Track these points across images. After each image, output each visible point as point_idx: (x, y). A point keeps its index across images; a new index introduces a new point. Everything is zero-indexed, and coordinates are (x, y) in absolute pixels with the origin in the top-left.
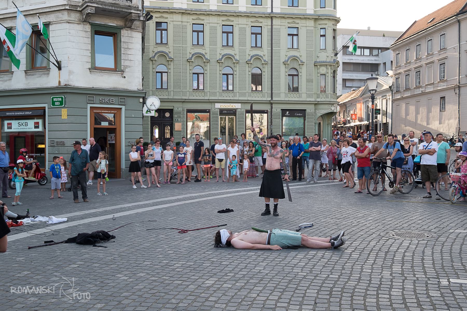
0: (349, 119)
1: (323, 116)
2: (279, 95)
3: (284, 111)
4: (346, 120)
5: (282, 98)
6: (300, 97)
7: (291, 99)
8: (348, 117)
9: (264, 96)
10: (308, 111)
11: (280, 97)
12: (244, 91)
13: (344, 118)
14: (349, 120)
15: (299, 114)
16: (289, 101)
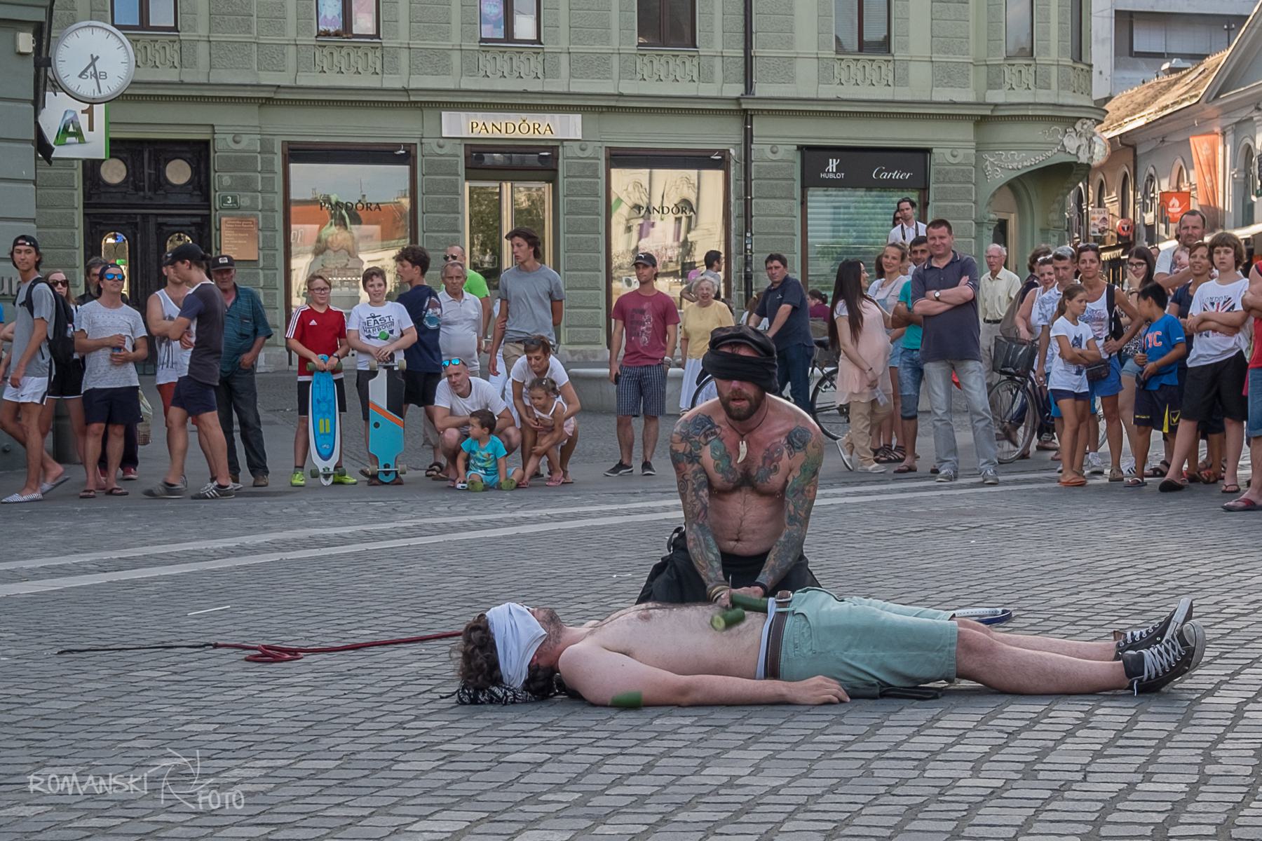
0: (1149, 218)
1: (1018, 186)
2: (786, 68)
3: (812, 156)
4: (1133, 227)
5: (805, 83)
6: (900, 79)
7: (848, 92)
8: (1145, 209)
9: (705, 76)
10: (941, 156)
11: (791, 79)
12: (598, 48)
13: (1124, 214)
14: (1150, 229)
15: (896, 175)
16: (838, 100)
